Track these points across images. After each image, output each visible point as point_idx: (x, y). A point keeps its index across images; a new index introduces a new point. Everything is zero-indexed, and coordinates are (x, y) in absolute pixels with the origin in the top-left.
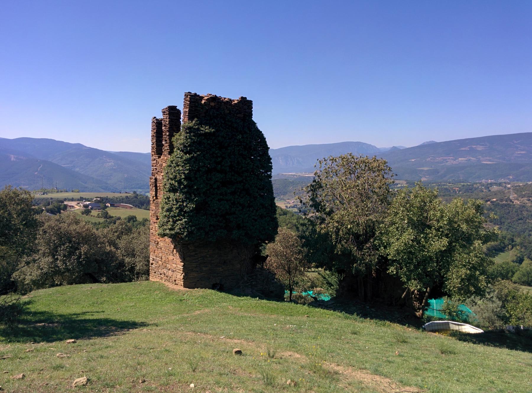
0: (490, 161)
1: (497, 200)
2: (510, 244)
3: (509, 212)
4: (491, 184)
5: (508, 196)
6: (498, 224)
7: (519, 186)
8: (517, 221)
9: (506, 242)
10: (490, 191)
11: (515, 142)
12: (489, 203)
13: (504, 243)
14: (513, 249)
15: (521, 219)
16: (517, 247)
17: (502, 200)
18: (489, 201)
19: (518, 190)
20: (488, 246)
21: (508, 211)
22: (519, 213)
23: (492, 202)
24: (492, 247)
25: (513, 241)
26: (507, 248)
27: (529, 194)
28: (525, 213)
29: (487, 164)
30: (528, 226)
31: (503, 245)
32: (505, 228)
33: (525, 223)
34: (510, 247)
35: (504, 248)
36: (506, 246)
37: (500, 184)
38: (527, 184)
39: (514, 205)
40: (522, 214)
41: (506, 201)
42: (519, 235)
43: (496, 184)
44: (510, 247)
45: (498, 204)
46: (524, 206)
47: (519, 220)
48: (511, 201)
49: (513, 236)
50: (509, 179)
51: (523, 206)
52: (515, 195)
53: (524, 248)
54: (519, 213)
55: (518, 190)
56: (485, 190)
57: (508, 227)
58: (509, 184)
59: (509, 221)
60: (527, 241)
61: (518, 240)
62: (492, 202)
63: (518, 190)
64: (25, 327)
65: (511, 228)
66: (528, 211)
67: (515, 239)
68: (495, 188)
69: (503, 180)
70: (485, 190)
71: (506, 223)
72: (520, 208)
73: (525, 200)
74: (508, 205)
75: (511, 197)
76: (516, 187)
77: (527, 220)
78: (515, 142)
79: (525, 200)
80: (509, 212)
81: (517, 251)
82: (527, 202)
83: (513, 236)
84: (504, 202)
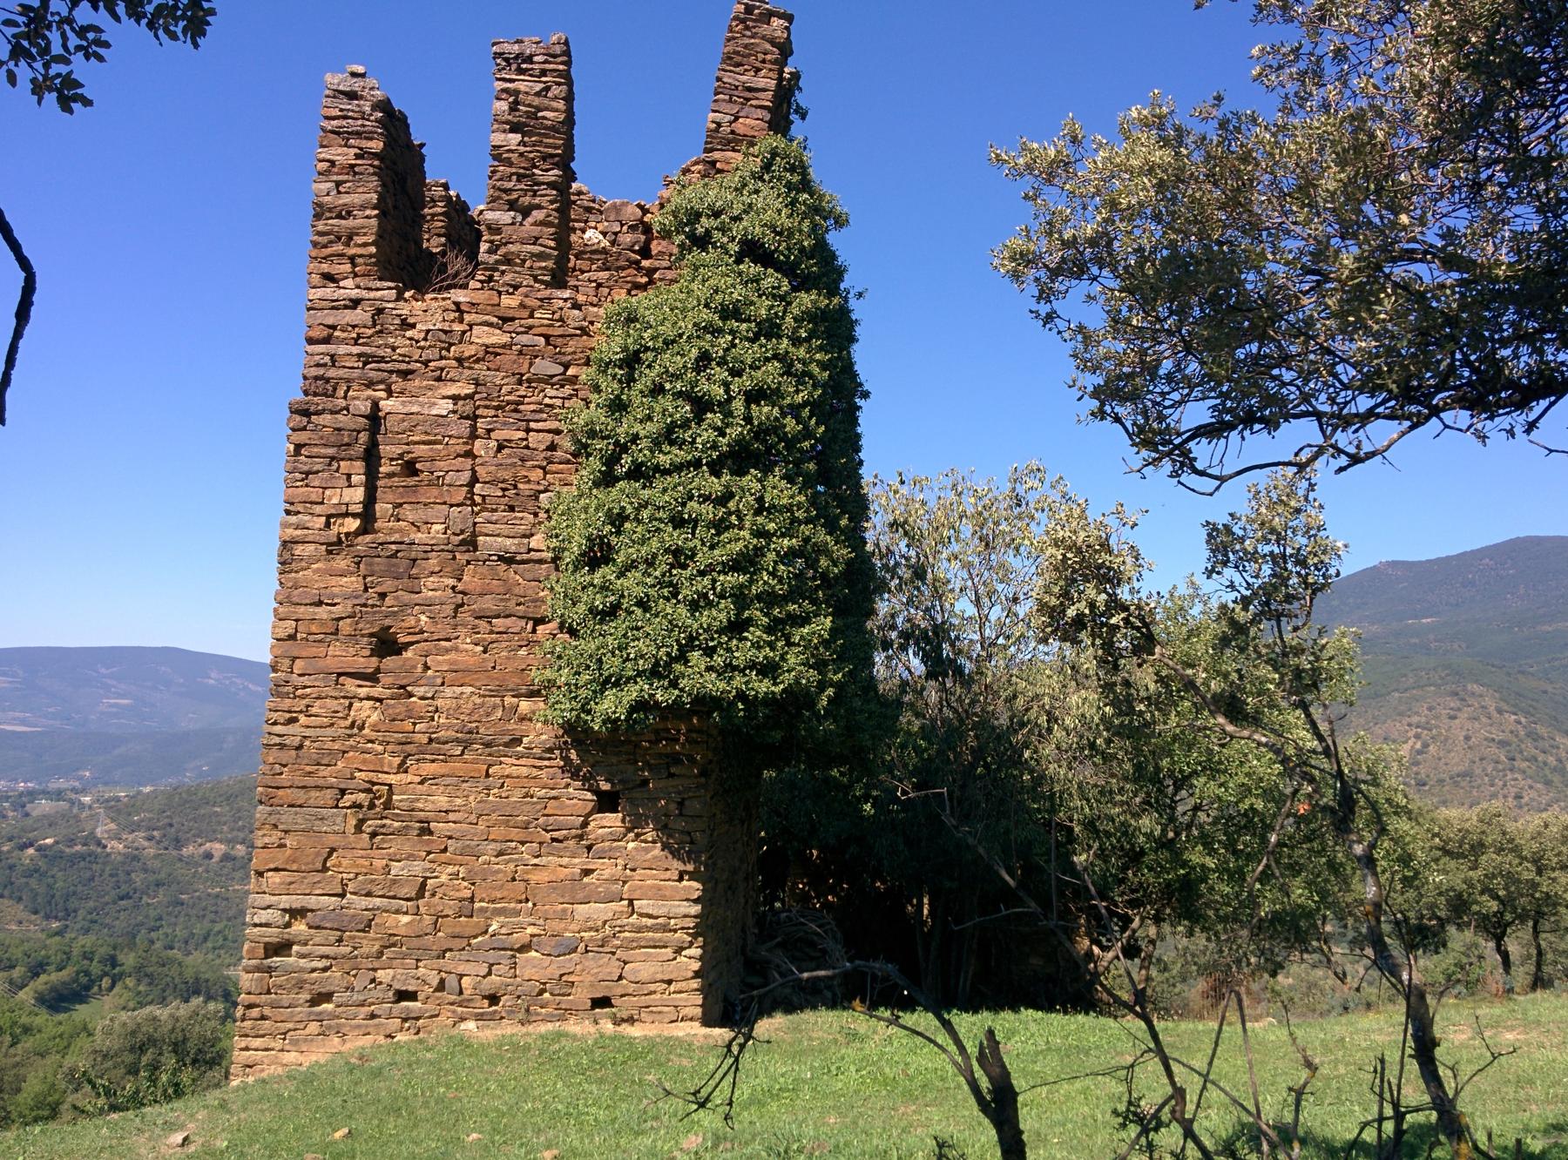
0: (23, 722)
1: (57, 843)
2: (106, 974)
3: (92, 879)
4: (32, 795)
5: (88, 828)
6: (56, 918)
7: (118, 799)
8: (115, 903)
9: (95, 968)
10: (27, 815)
11: (103, 671)
12: (31, 851)
13: (87, 973)
14: (116, 990)
15: (126, 897)
16: (128, 980)
17: (71, 842)
18: (31, 845)
19: (115, 809)
20: (41, 988)
21: (88, 874)
22: (122, 877)
23: (39, 849)
24: (53, 989)
25: (113, 962)
26: (96, 989)
27: (150, 819)
28: (138, 878)
29: (14, 733)
30: (147, 917)
31: (84, 980)
32: (78, 926)
33: (136, 907)
34: (106, 982)
35: (88, 988)
36: (92, 982)
37: (58, 795)
38: (139, 793)
39: (108, 855)
40: (130, 882)
41: (85, 845)
42: (132, 945)
43: (46, 793)
44: (106, 982)
45: (60, 856)
46: (135, 858)
47: (122, 899)
48: (99, 843)
49: (115, 948)
50: (80, 778)
51: (134, 857)
52: (113, 826)
53: (146, 980)
54: (122, 877)
55: (115, 809)
56: (11, 814)
57: (87, 924)
58: (84, 791)
59: (91, 904)
60: (154, 959)
61: (128, 960)
62: (39, 849)
63: (119, 811)
64: (291, 1057)
65: (96, 927)
66: (146, 871)
67: (121, 958)
68: (44, 806)
69: (62, 784)
70: (11, 814)
71: (81, 913)
72: (124, 863)
73: (139, 838)
74: (91, 857)
75: (99, 832)
76: (107, 801)
77: (145, 898)
78: (103, 671)
79: (139, 838)
80: (92, 879)
81: (127, 994)
82: (146, 844)
83: (115, 948)
84: (79, 848)
